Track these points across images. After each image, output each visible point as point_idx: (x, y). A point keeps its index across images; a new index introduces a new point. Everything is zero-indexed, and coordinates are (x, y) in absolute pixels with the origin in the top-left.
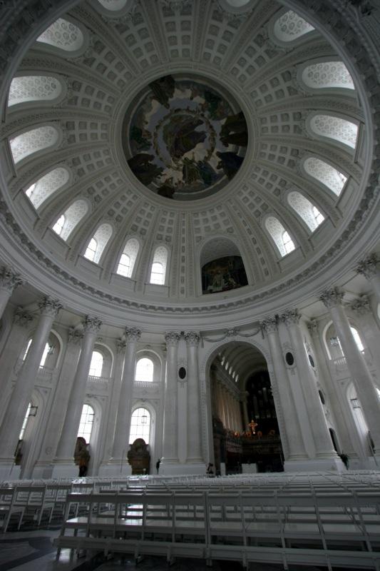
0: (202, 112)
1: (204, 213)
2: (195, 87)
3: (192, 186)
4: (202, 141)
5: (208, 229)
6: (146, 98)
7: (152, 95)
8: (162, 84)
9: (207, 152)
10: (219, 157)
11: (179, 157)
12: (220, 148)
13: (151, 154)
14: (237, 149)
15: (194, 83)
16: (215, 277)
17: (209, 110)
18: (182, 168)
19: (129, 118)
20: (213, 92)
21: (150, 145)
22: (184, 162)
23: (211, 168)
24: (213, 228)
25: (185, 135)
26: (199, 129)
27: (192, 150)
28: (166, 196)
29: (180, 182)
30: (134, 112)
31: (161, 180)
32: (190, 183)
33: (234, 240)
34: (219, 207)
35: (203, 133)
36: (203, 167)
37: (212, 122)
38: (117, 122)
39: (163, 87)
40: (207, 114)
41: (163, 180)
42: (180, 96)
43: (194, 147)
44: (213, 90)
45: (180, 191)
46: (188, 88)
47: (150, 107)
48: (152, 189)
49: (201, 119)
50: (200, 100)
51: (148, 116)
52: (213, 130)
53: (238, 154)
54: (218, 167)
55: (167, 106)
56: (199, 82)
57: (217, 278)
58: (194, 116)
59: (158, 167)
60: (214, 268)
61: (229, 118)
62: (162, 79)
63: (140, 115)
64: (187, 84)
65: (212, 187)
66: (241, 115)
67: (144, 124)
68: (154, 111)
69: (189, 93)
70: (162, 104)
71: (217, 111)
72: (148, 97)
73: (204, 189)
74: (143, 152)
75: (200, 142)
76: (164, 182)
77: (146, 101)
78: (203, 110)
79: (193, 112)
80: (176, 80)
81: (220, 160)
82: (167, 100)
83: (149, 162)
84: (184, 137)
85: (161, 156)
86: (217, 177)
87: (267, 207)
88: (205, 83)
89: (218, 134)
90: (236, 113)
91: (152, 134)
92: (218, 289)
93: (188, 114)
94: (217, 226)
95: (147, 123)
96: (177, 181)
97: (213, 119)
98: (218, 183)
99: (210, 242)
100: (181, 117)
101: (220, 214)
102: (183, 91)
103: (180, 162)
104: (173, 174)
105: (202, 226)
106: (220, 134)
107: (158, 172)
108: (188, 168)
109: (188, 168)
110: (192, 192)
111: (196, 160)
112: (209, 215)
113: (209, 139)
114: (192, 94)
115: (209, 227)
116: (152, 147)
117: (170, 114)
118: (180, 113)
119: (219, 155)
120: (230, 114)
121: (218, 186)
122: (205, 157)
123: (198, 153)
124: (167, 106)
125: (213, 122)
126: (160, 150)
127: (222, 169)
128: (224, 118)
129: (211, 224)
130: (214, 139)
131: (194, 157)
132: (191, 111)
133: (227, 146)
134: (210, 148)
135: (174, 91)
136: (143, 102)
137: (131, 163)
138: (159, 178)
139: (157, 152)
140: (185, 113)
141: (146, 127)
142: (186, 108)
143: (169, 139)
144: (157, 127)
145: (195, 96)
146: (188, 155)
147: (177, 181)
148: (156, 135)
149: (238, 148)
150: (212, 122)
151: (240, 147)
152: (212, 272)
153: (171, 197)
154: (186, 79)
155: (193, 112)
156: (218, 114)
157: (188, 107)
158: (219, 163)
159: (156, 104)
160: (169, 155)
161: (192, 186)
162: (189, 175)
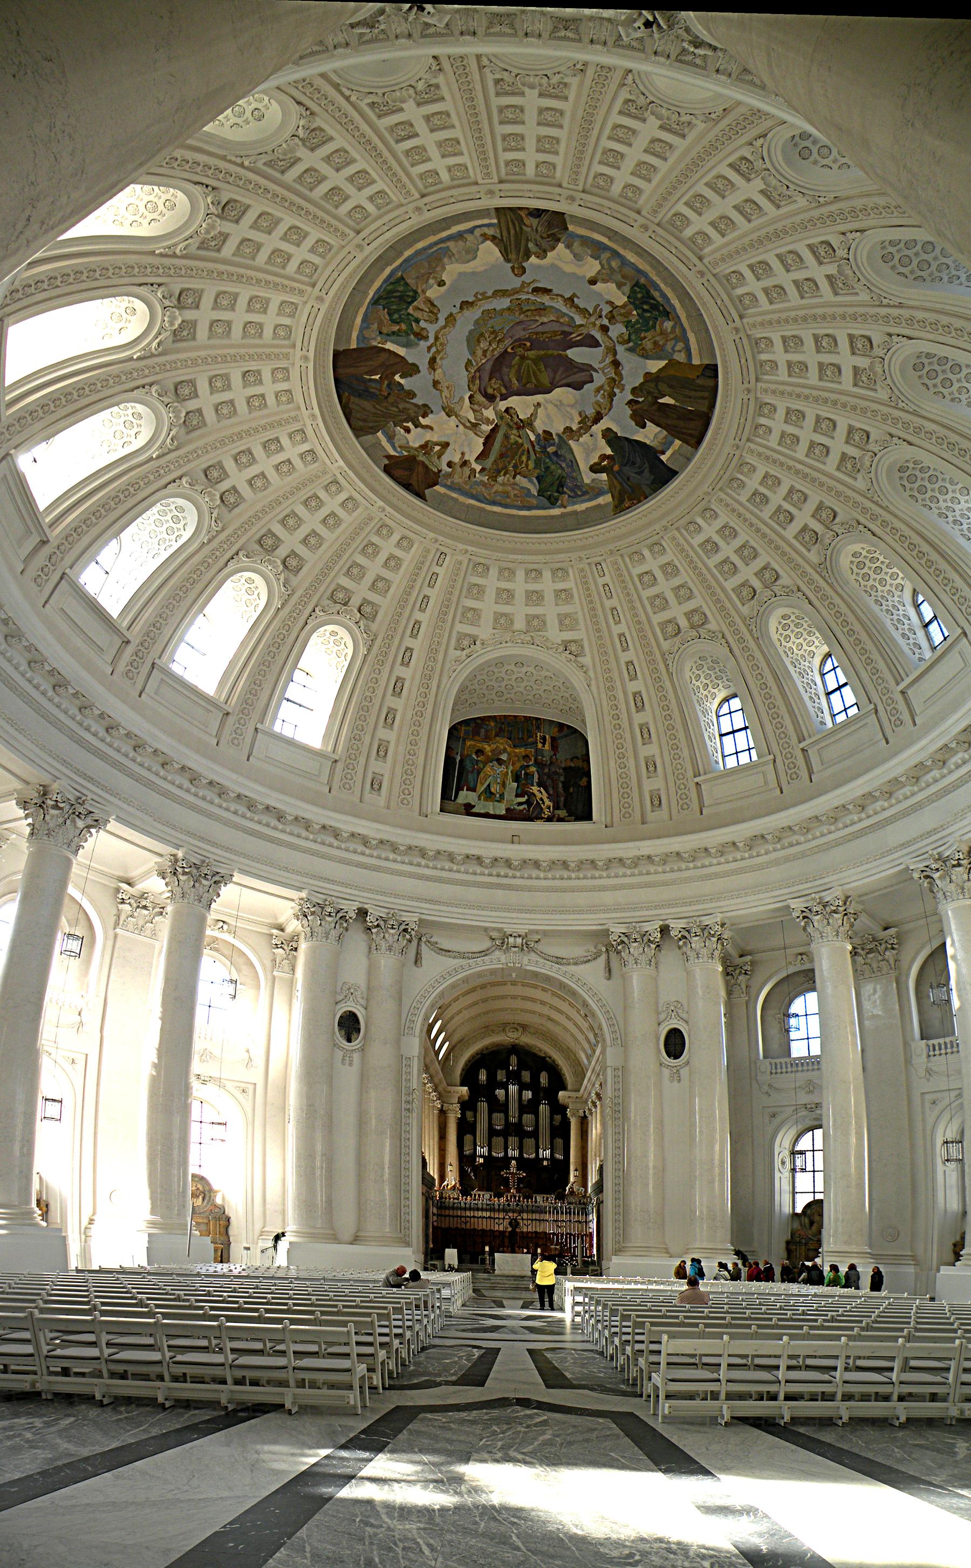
0: (605, 322)
1: (507, 573)
3: (497, 488)
4: (578, 386)
5: (503, 621)
9: (577, 419)
10: (609, 443)
11: (491, 398)
12: (619, 420)
15: (616, 254)
16: (488, 769)
17: (628, 324)
18: (487, 428)
20: (656, 294)
22: (502, 418)
23: (573, 464)
24: (520, 624)
25: (531, 354)
27: (539, 398)
32: (494, 478)
34: (559, 572)
36: (551, 449)
39: (526, 230)
40: (617, 330)
49: (598, 336)
50: (614, 293)
52: (618, 373)
54: (594, 469)
56: (631, 257)
57: (493, 774)
58: (579, 320)
60: (487, 739)
61: (672, 363)
62: (537, 213)
64: (597, 249)
65: (556, 512)
66: (712, 370)
69: (592, 267)
71: (649, 335)
73: (529, 508)
75: (568, 385)
79: (583, 312)
80: (571, 228)
81: (609, 451)
84: (528, 355)
89: (628, 388)
90: (696, 361)
92: (491, 808)
93: (564, 310)
94: (536, 624)
97: (630, 350)
99: (499, 662)
100: (542, 309)
101: (558, 593)
106: (634, 391)
108: (506, 437)
109: (506, 437)
110: (494, 503)
111: (539, 425)
113: (598, 390)
115: (509, 618)
118: (545, 299)
119: (609, 436)
120: (681, 357)
121: (575, 513)
122: (568, 429)
123: (552, 411)
125: (627, 354)
129: (520, 611)
130: (612, 395)
131: (534, 415)
132: (577, 307)
134: (590, 412)
135: (553, 248)
140: (560, 305)
142: (567, 295)
145: (605, 281)
146: (521, 405)
152: (479, 752)
155: (583, 312)
156: (648, 345)
157: (574, 295)
158: (603, 457)
161: (497, 488)
162: (502, 456)
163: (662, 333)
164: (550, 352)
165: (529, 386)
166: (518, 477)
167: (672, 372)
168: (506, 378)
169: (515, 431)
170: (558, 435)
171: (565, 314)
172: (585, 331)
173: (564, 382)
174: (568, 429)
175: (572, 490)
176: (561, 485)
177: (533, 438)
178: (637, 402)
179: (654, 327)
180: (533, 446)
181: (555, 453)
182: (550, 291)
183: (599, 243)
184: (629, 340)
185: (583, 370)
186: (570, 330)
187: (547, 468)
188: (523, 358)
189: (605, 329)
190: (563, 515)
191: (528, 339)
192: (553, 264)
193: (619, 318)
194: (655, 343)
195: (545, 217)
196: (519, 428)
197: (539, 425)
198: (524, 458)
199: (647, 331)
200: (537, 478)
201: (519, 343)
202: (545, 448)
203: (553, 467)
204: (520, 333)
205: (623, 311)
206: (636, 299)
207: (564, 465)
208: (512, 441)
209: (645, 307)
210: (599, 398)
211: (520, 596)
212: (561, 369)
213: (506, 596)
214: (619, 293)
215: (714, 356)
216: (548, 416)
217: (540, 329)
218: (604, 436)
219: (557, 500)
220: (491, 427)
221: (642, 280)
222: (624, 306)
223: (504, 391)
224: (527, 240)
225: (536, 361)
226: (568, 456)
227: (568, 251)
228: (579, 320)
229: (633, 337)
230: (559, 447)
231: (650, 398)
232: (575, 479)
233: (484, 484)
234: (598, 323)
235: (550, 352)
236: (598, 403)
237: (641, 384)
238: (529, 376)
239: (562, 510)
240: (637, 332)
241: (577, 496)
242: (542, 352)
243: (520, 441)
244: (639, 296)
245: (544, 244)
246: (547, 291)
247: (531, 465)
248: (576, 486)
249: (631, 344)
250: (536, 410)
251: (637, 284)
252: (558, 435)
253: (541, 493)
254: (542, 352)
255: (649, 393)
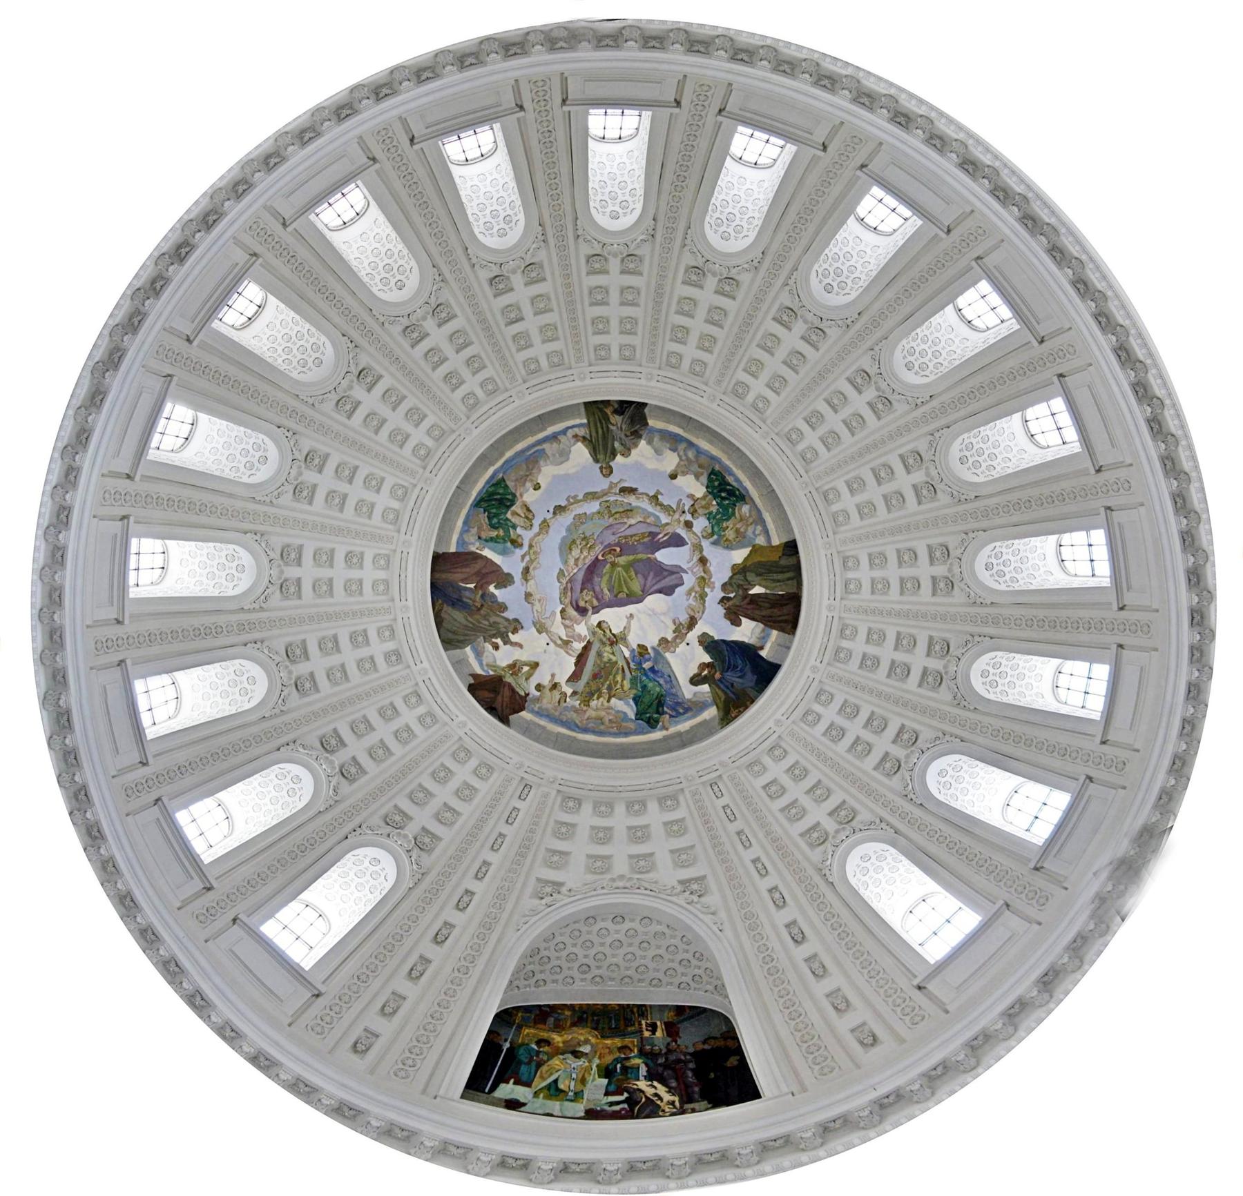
0: (689, 517)
2: (691, 454)
3: (591, 713)
4: (668, 591)
5: (599, 864)
6: (564, 432)
7: (582, 432)
8: (616, 419)
11: (582, 611)
12: (715, 624)
13: (506, 571)
14: (764, 638)
15: (691, 444)
17: (709, 516)
18: (578, 646)
19: (502, 454)
20: (730, 479)
21: (516, 543)
22: (594, 633)
23: (671, 679)
24: (621, 866)
25: (622, 560)
26: (665, 556)
27: (631, 608)
28: (491, 709)
29: (555, 686)
30: (520, 446)
31: (497, 654)
32: (586, 702)
33: (702, 927)
34: (668, 800)
35: (676, 571)
36: (647, 665)
37: (709, 550)
38: (475, 439)
39: (615, 423)
40: (700, 524)
41: (503, 657)
42: (644, 461)
43: (640, 601)
44: (731, 474)
45: (539, 714)
46: (674, 450)
47: (564, 455)
48: (459, 664)
49: (682, 532)
50: (694, 487)
51: (547, 473)
53: (763, 653)
54: (695, 681)
55: (608, 471)
56: (704, 445)
58: (664, 519)
59: (509, 615)
61: (756, 550)
62: (623, 407)
63: (531, 461)
64: (674, 441)
65: (657, 735)
67: (528, 484)
68: (569, 467)
70: (597, 461)
71: (730, 523)
72: (570, 433)
73: (627, 734)
74: (487, 553)
75: (660, 591)
76: (504, 664)
77: (562, 438)
78: (694, 513)
79: (667, 509)
80: (651, 422)
81: (707, 659)
82: (614, 455)
83: (492, 588)
85: (531, 586)
86: (683, 709)
87: (854, 813)
88: (715, 452)
89: (718, 585)
91: (536, 523)
93: (650, 509)
94: (643, 863)
95: (537, 487)
96: (546, 682)
97: (714, 543)
98: (684, 726)
100: (629, 511)
102: (658, 452)
103: (582, 629)
104: (542, 652)
105: (580, 848)
106: (724, 587)
107: (504, 630)
108: (599, 655)
109: (599, 655)
110: (585, 730)
111: (634, 640)
112: (620, 820)
113: (689, 593)
114: (678, 465)
116: (519, 552)
117: (605, 494)
118: (631, 500)
119: (709, 644)
121: (679, 734)
122: (663, 641)
123: (643, 622)
124: (608, 471)
125: (713, 548)
126: (534, 579)
127: (706, 688)
128: (744, 546)
129: (620, 852)
130: (702, 597)
132: (661, 505)
133: (736, 623)
134: (684, 618)
135: (636, 446)
136: (554, 437)
137: (440, 561)
138: (496, 647)
139: (526, 571)
141: (529, 496)
143: (576, 552)
144: (559, 509)
145: (684, 473)
146: (614, 617)
147: (546, 682)
148: (545, 525)
149: (768, 635)
150: (709, 550)
151: (775, 633)
153: (504, 720)
154: (673, 429)
155: (667, 509)
157: (658, 492)
158: (703, 666)
159: (581, 453)
160: (557, 595)
162: (595, 676)
163: (741, 520)
164: (640, 556)
165: (621, 595)
166: (613, 700)
167: (758, 559)
168: (597, 588)
169: (608, 648)
170: (653, 648)
171: (650, 514)
172: (670, 530)
173: (655, 588)
174: (663, 641)
175: (673, 709)
176: (660, 704)
177: (627, 654)
178: (729, 599)
179: (734, 514)
180: (628, 664)
181: (652, 669)
182: (636, 490)
183: (676, 435)
184: (713, 534)
185: (673, 573)
186: (657, 530)
187: (644, 687)
188: (614, 565)
189: (688, 525)
190: (665, 738)
191: (618, 544)
192: (637, 463)
193: (700, 511)
194: (737, 531)
195: (628, 414)
196: (612, 644)
197: (634, 640)
198: (619, 678)
199: (727, 520)
200: (634, 699)
201: (609, 549)
202: (640, 664)
203: (650, 685)
204: (612, 539)
205: (704, 503)
206: (714, 487)
207: (662, 681)
208: (605, 659)
209: (723, 495)
210: (691, 601)
211: (620, 833)
212: (652, 574)
213: (603, 835)
214: (699, 484)
215: (791, 531)
216: (642, 628)
217: (628, 532)
218: (701, 643)
219: (657, 722)
220: (583, 644)
221: (717, 468)
222: (704, 498)
223: (595, 603)
224: (614, 440)
225: (626, 568)
226: (666, 671)
227: (649, 447)
228: (664, 519)
229: (716, 529)
230: (656, 661)
231: (741, 592)
232: (675, 695)
233: (576, 711)
234: (682, 519)
235: (640, 556)
236: (689, 607)
237: (731, 578)
238: (620, 585)
239: (664, 733)
240: (719, 522)
241: (679, 714)
242: (631, 558)
243: (614, 659)
244: (716, 483)
245: (627, 440)
246: (632, 491)
247: (627, 684)
248: (678, 704)
249: (715, 537)
250: (629, 623)
251: (713, 472)
252: (653, 648)
253: (639, 715)
254: (631, 558)
255: (739, 586)
